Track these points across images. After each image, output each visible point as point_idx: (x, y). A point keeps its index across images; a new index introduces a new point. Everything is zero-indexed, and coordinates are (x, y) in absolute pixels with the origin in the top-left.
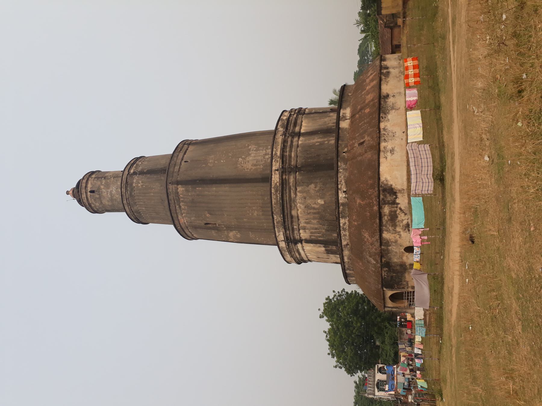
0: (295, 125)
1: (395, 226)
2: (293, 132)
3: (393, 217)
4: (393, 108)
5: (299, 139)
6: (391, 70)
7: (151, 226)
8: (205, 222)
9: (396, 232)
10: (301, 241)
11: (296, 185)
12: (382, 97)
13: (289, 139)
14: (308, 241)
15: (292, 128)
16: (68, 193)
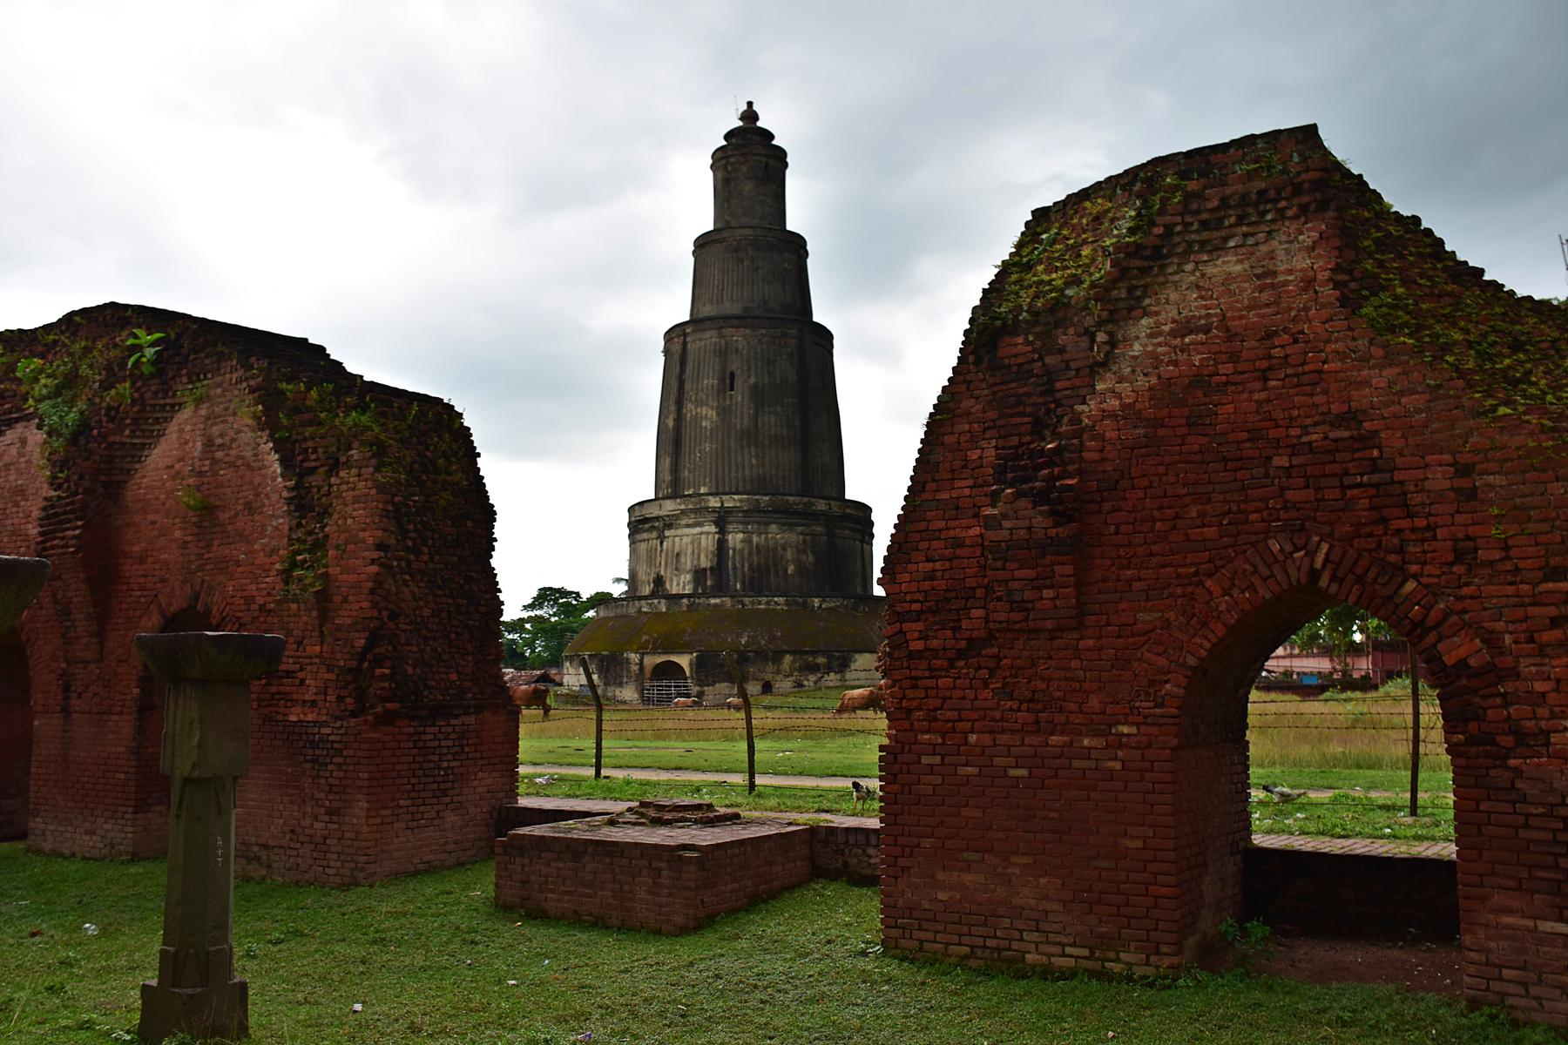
1: (801, 670)
3: (813, 668)
7: (692, 259)
8: (738, 373)
9: (792, 670)
10: (722, 531)
11: (814, 535)
14: (722, 545)
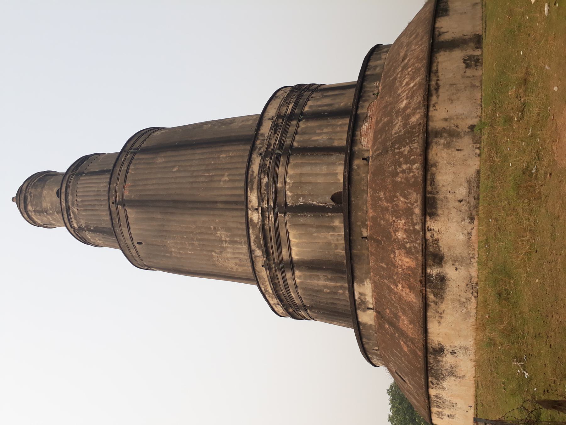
0: (279, 247)
2: (281, 262)
4: (451, 374)
5: (293, 273)
6: (449, 271)
12: (431, 350)
13: (279, 275)
15: (276, 254)
16: (13, 199)
